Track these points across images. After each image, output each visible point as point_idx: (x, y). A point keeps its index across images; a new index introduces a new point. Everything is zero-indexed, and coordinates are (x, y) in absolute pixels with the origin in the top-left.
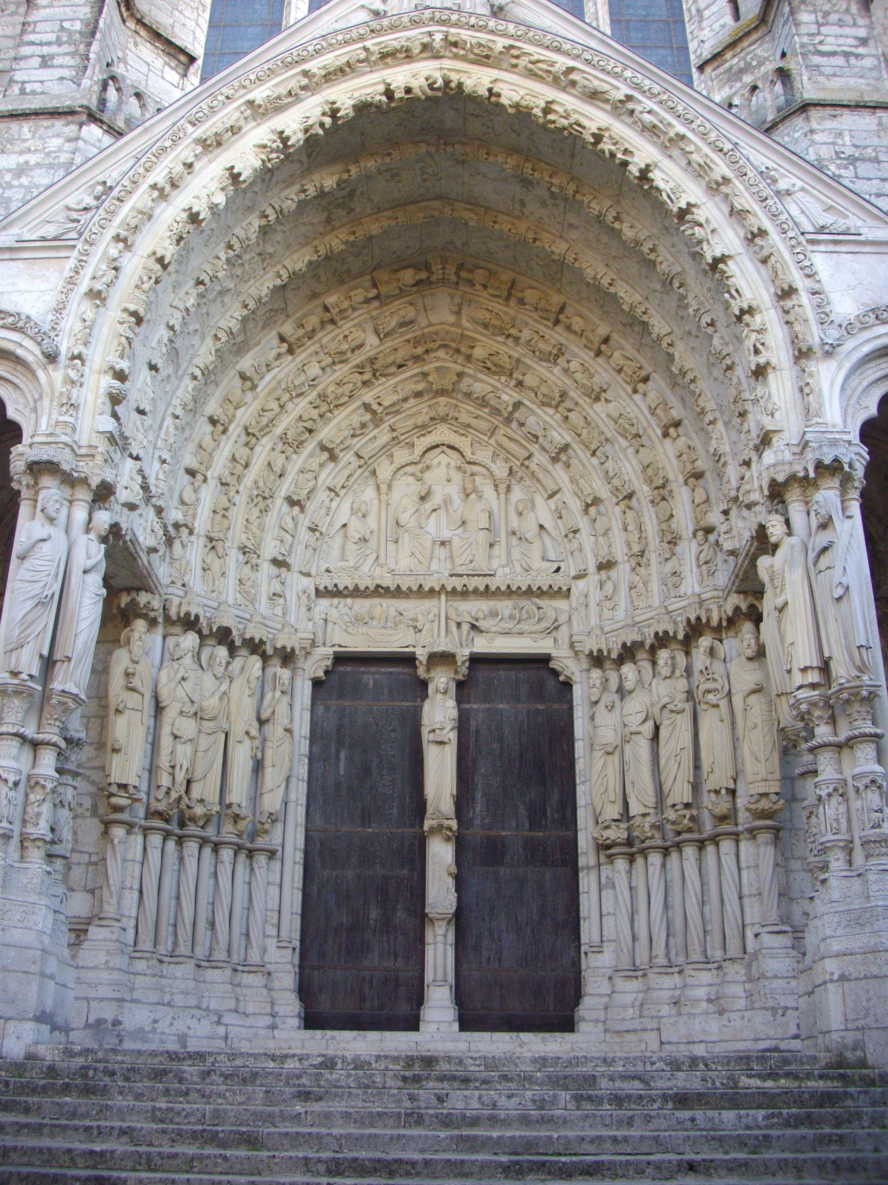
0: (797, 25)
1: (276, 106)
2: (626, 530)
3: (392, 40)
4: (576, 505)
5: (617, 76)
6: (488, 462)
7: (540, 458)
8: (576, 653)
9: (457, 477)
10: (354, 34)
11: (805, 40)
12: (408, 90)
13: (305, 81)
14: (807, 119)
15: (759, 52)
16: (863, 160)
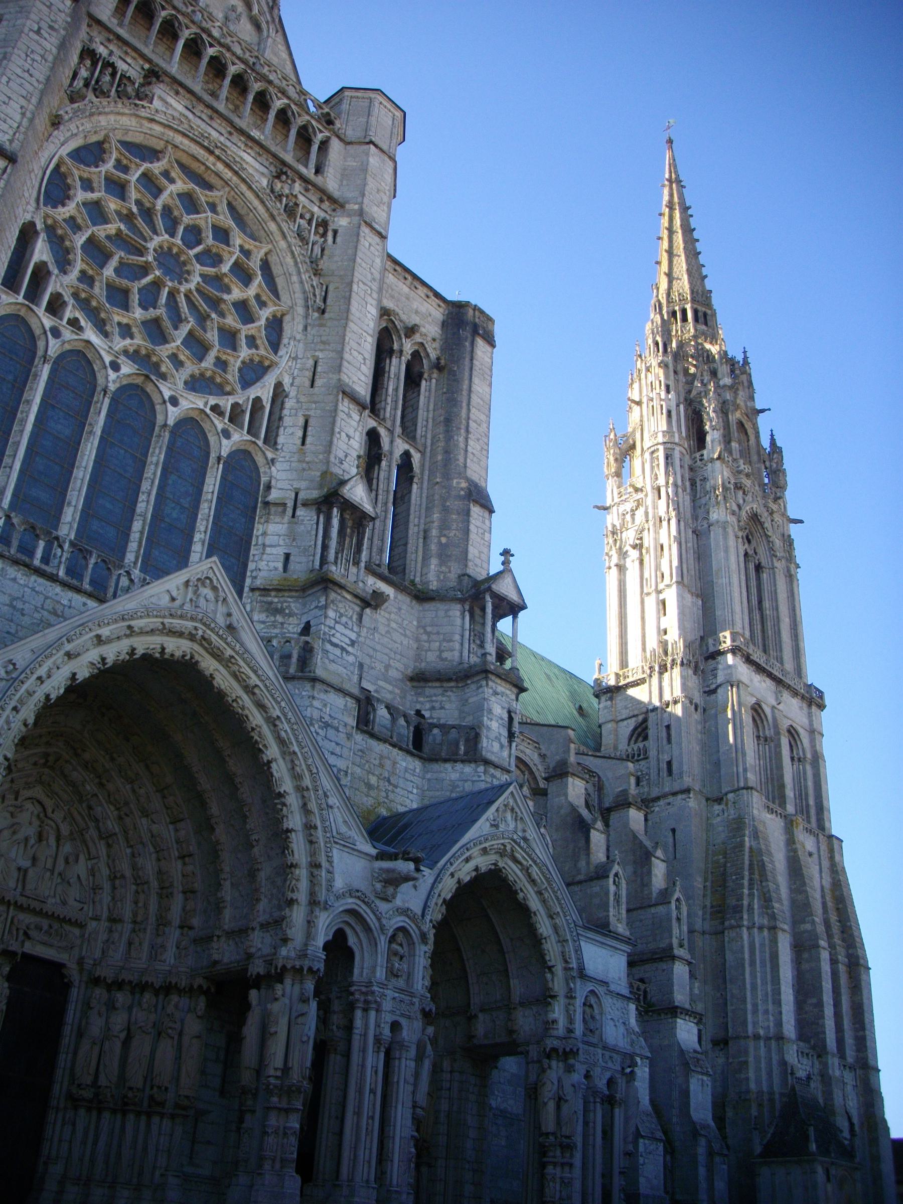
0: (326, 617)
1: (109, 641)
2: (136, 903)
3: (176, 623)
4: (105, 871)
5: (278, 703)
6: (59, 821)
7: (92, 832)
8: (81, 970)
9: (36, 823)
10: (162, 613)
11: (327, 630)
12: (172, 655)
13: (128, 632)
14: (313, 687)
15: (292, 605)
16: (332, 727)
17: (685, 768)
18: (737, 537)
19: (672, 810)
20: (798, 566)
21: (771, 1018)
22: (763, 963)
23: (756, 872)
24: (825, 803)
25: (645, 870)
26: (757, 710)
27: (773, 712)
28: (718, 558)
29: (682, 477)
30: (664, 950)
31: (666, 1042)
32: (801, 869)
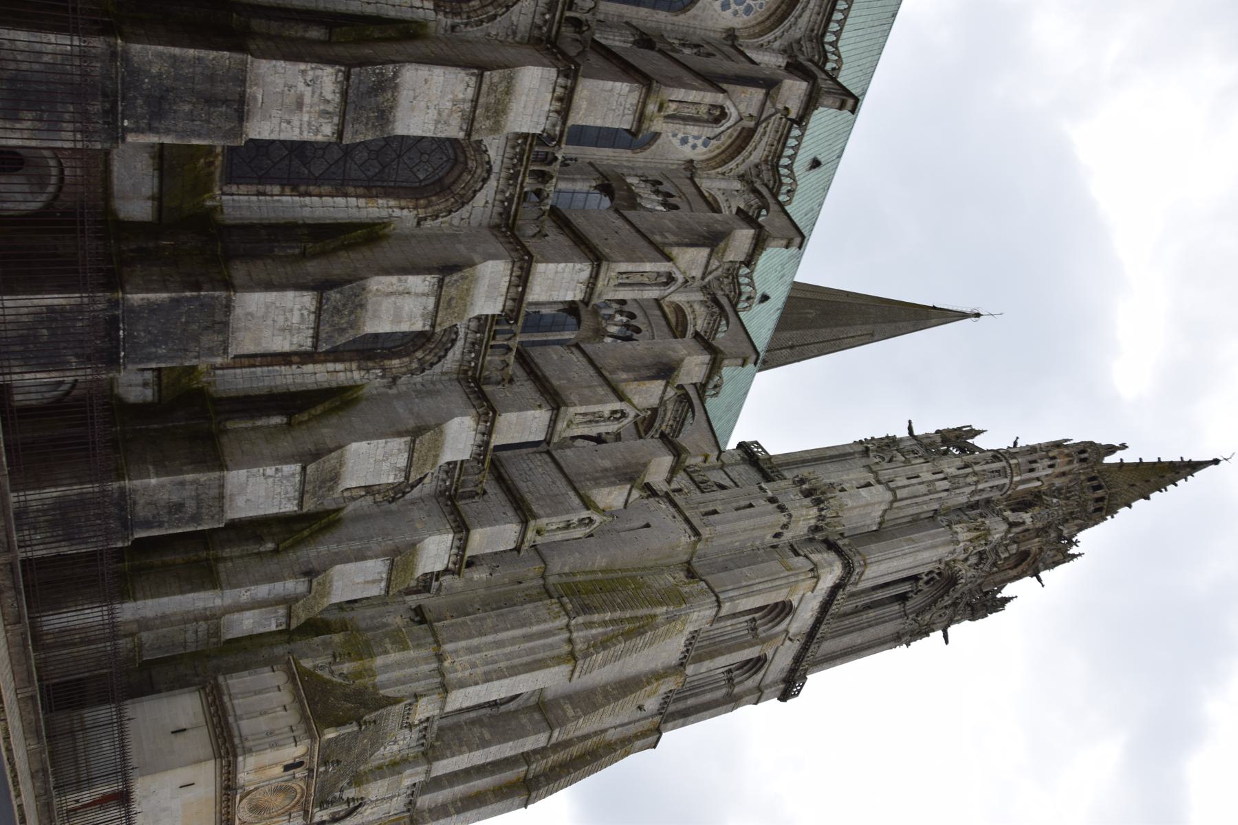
17: (718, 528)
18: (940, 561)
19: (669, 519)
20: (908, 645)
21: (467, 673)
22: (532, 651)
23: (632, 626)
24: (692, 718)
25: (613, 479)
26: (784, 610)
27: (781, 632)
28: (925, 537)
29: (983, 490)
30: (530, 510)
31: (418, 525)
32: (632, 692)
